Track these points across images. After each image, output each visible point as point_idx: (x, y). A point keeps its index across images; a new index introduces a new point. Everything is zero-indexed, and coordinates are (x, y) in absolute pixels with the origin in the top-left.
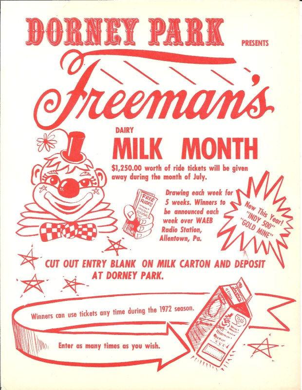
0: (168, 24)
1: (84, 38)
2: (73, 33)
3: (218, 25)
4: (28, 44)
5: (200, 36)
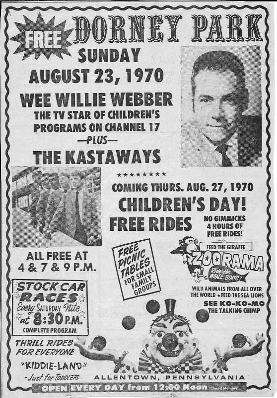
0: (210, 21)
1: (128, 36)
2: (117, 30)
5: (240, 33)
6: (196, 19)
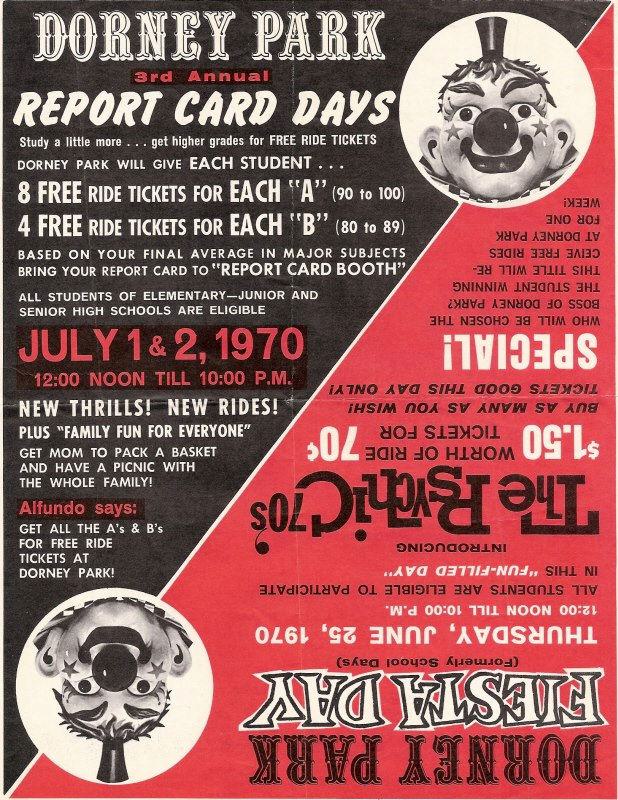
5: (292, 754)
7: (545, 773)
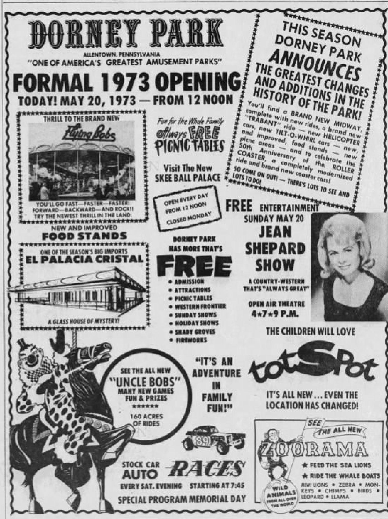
1: (85, 40)
2: (74, 35)
3: (218, 26)
4: (31, 47)
6: (155, 23)
7: (60, 27)
